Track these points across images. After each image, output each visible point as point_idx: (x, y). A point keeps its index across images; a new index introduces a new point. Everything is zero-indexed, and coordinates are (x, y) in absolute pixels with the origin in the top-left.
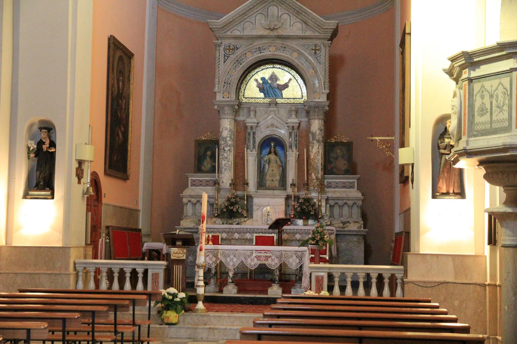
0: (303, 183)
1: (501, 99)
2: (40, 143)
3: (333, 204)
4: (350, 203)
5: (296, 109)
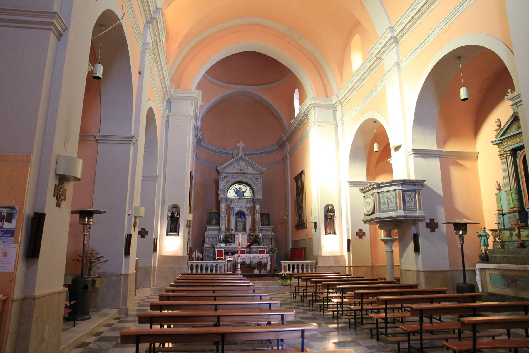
0: (253, 229)
1: (392, 199)
2: (173, 214)
3: (265, 237)
4: (270, 237)
5: (248, 201)
